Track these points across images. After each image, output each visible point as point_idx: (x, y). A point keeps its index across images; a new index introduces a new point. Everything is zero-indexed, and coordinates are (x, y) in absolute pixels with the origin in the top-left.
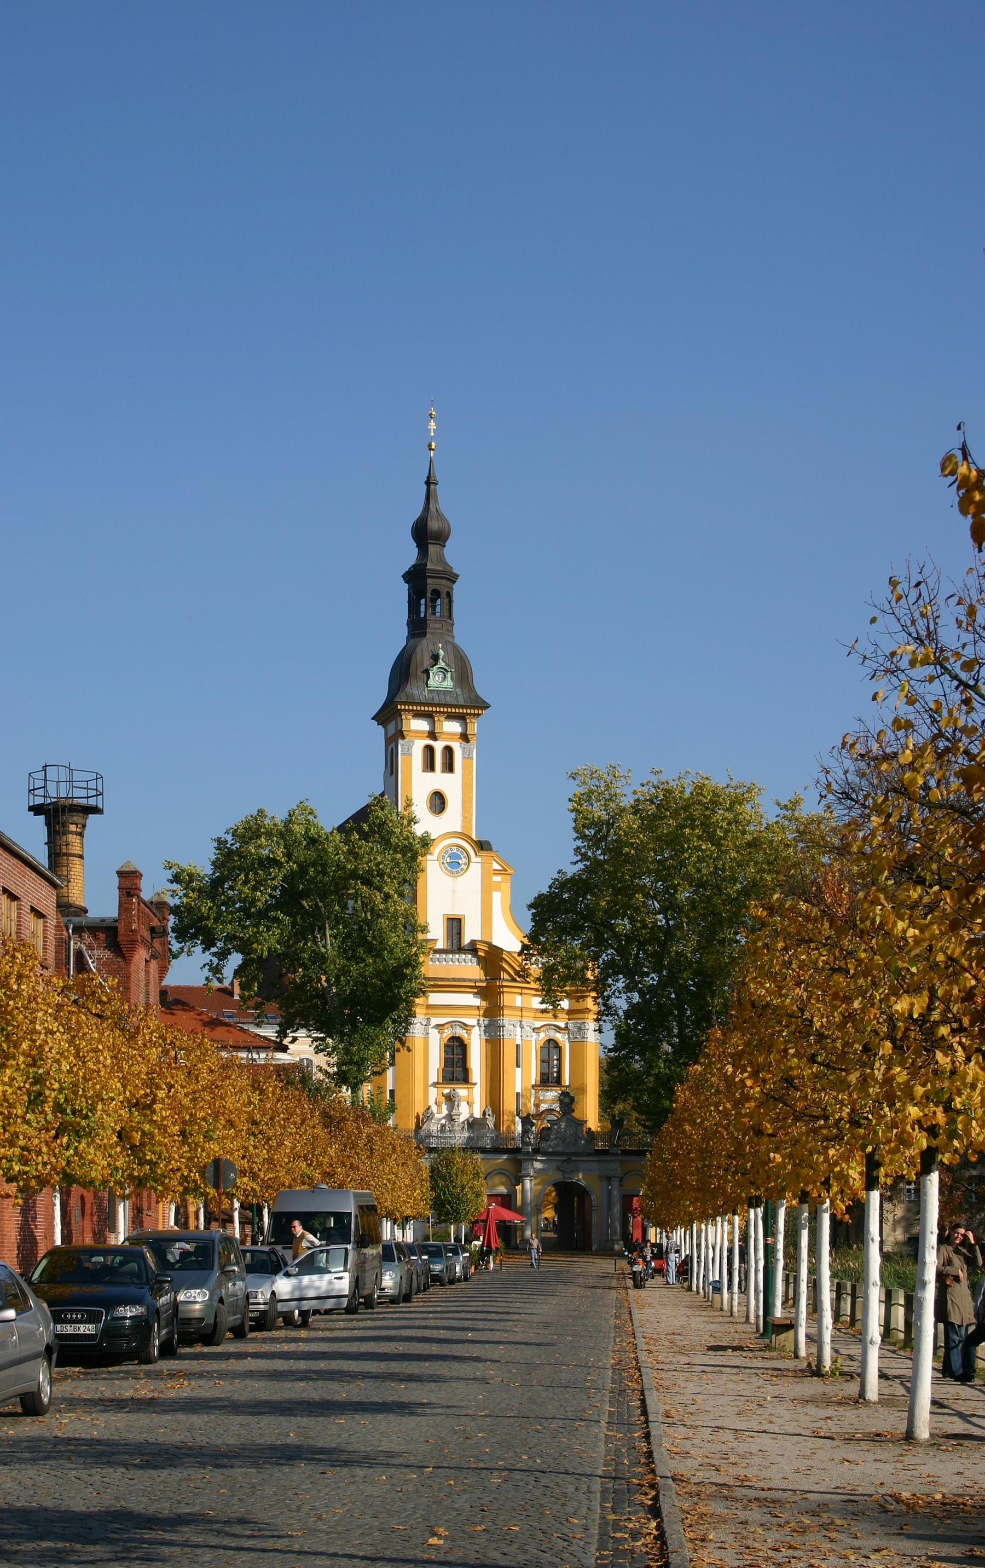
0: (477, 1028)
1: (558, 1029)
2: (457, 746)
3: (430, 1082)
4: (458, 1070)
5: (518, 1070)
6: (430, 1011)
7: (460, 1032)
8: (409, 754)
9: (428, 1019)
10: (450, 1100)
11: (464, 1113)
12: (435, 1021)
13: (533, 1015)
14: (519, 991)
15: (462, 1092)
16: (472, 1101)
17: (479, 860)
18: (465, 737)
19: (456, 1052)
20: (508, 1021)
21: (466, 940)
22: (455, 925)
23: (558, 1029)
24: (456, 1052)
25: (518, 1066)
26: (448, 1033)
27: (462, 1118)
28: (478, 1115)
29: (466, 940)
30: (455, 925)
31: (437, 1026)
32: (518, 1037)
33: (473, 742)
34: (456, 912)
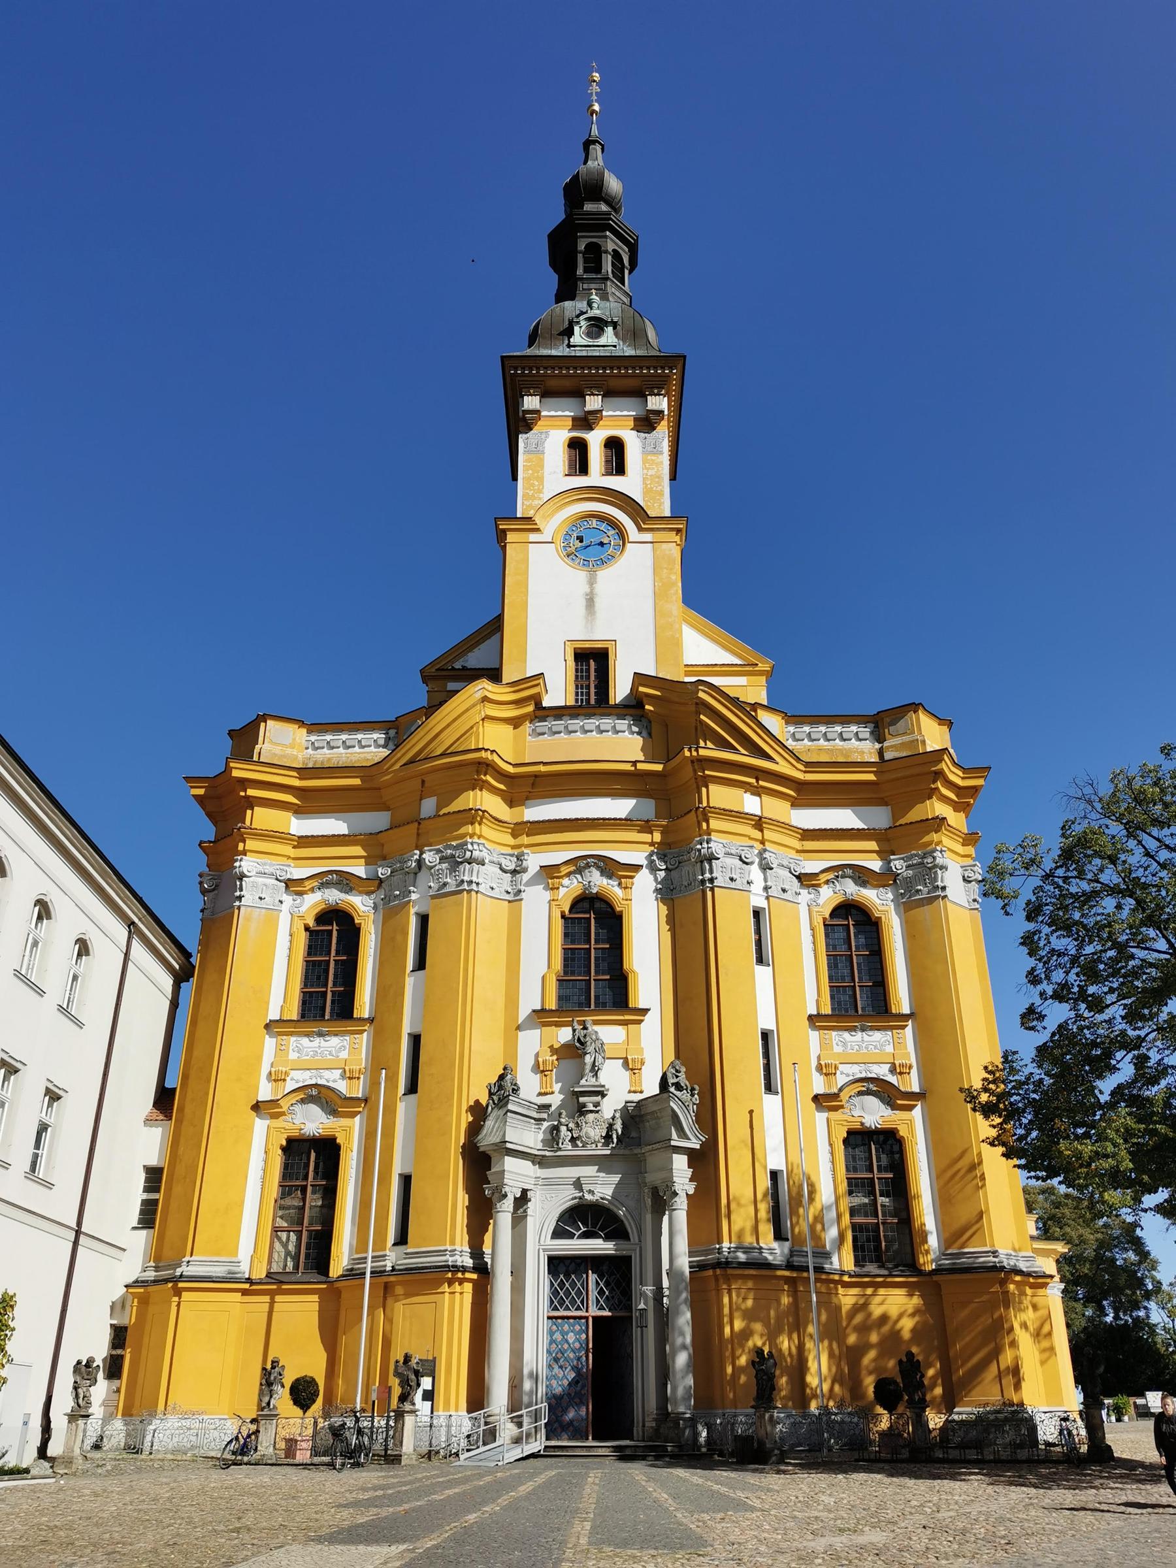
0: (645, 872)
1: (862, 876)
2: (633, 441)
3: (524, 1012)
4: (596, 978)
5: (763, 974)
6: (525, 840)
7: (598, 881)
8: (538, 451)
9: (519, 858)
10: (574, 1052)
11: (618, 1090)
12: (534, 861)
13: (797, 844)
15: (610, 1034)
16: (635, 1058)
17: (648, 537)
18: (646, 423)
19: (593, 932)
20: (722, 841)
21: (620, 689)
22: (593, 661)
23: (862, 876)
25: (760, 960)
26: (570, 887)
27: (610, 1107)
28: (651, 1087)
29: (620, 689)
30: (593, 661)
33: (663, 432)
34: (597, 634)
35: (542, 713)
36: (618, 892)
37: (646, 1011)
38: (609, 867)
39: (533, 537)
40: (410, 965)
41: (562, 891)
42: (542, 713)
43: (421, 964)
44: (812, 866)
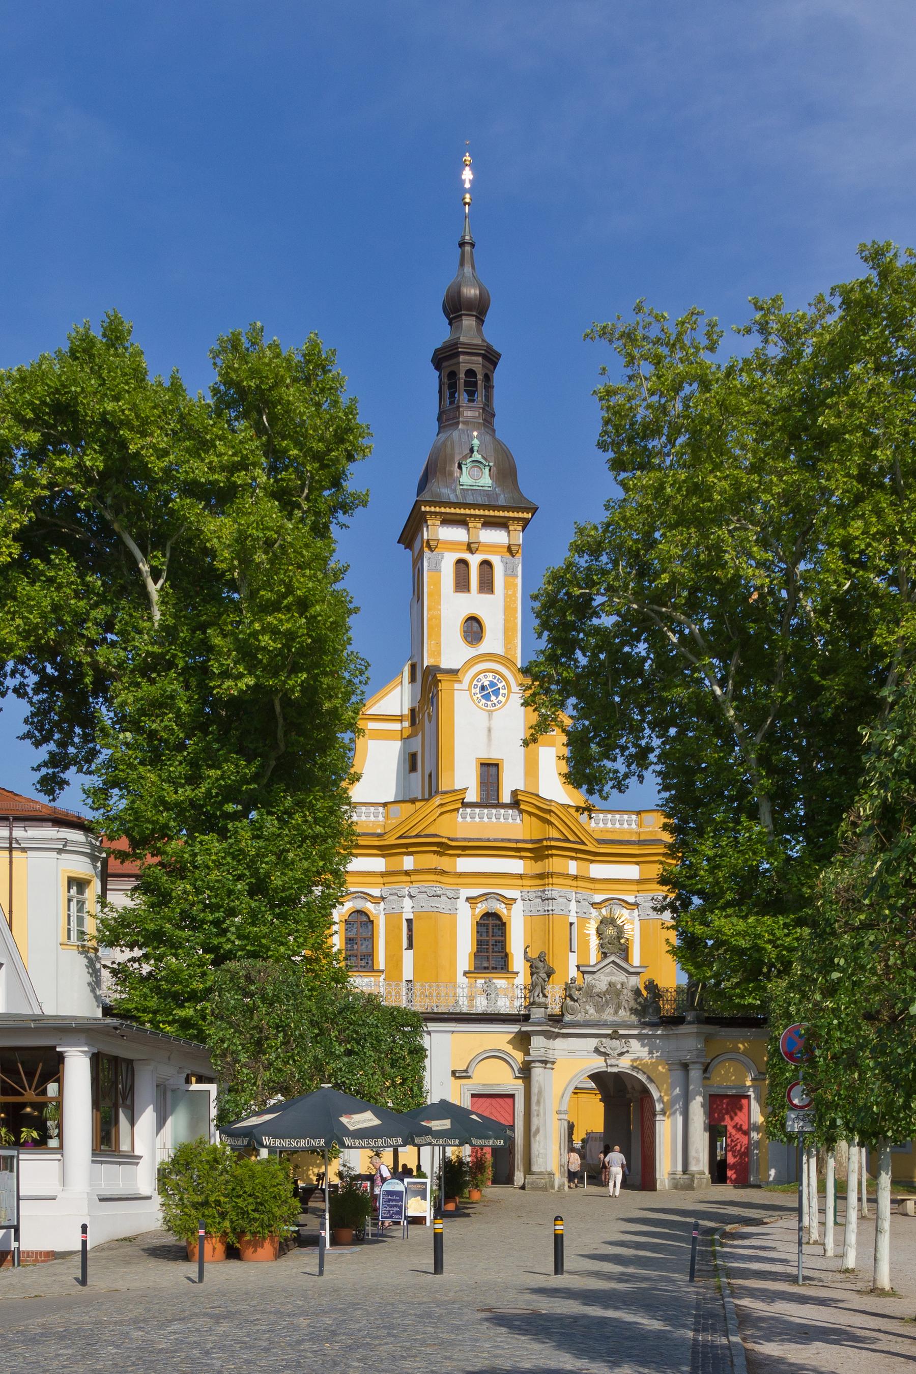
12: (465, 893)
14: (573, 854)
15: (500, 982)
19: (491, 931)
22: (490, 771)
24: (491, 931)
26: (481, 908)
30: (490, 771)
31: (468, 899)
32: (573, 913)
34: (494, 755)
35: (465, 805)
36: (505, 911)
37: (517, 973)
38: (501, 898)
39: (456, 686)
40: (405, 944)
41: (477, 910)
42: (465, 805)
43: (410, 946)
44: (598, 898)
